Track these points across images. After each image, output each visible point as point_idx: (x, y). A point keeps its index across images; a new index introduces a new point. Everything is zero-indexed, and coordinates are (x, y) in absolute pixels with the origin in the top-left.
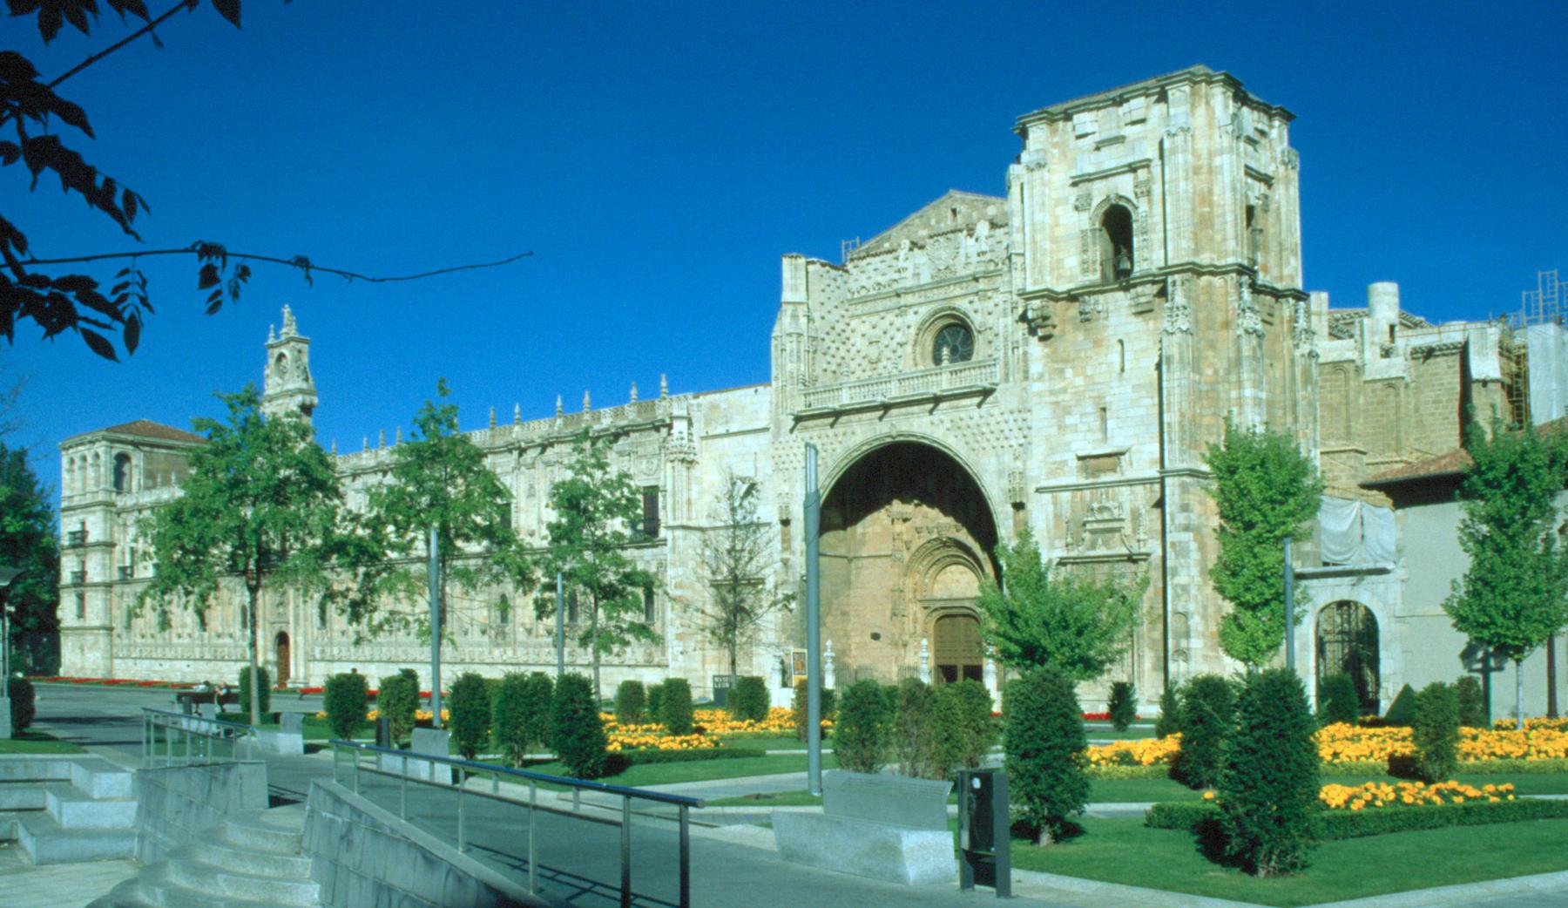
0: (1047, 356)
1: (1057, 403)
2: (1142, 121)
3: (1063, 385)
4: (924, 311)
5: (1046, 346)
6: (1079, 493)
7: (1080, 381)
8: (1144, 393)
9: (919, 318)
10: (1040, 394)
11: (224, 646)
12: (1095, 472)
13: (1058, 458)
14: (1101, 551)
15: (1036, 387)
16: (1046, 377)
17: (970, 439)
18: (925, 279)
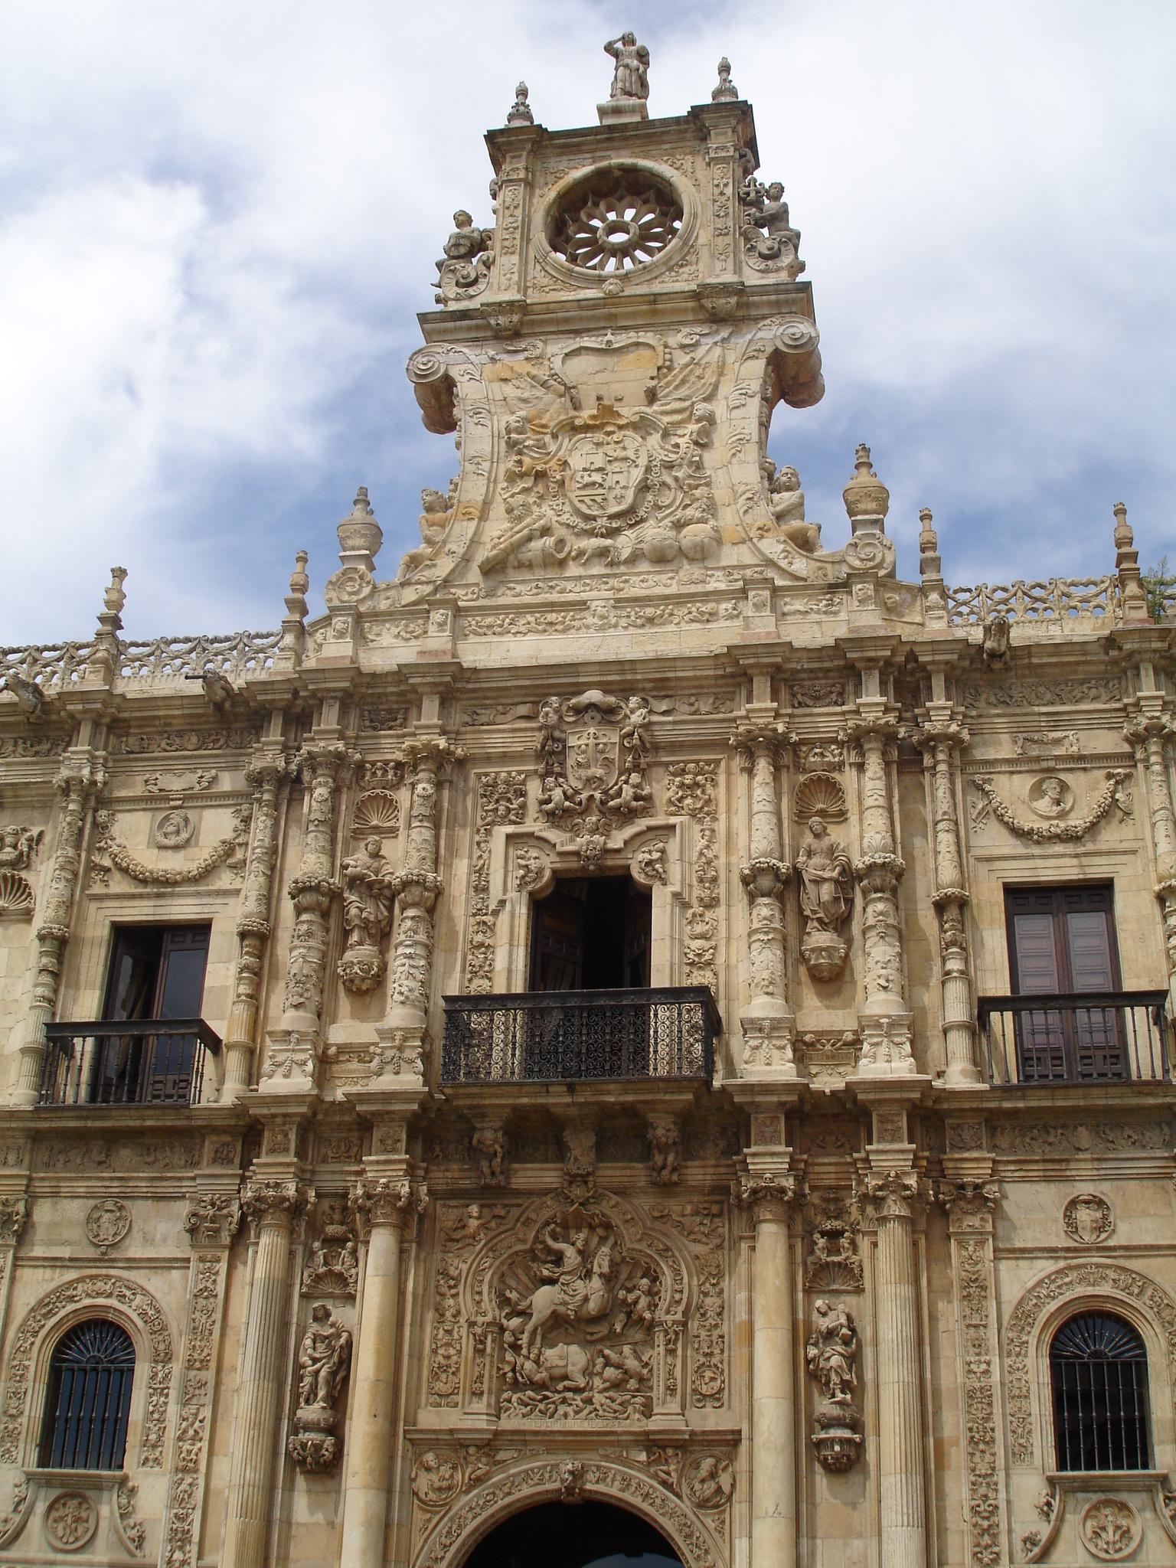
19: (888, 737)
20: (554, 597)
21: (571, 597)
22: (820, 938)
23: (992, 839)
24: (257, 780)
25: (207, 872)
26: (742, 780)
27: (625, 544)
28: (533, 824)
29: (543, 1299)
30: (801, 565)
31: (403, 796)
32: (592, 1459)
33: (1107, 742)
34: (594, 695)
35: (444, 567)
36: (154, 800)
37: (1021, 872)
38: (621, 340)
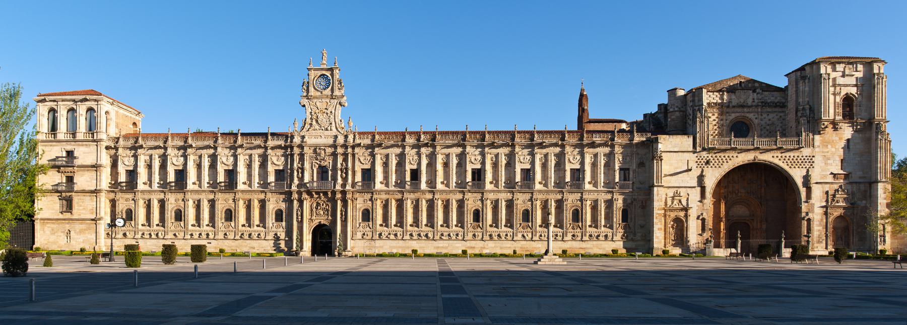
0: (821, 140)
1: (825, 156)
3: (827, 150)
4: (733, 116)
5: (821, 137)
6: (832, 185)
7: (833, 150)
8: (857, 156)
9: (731, 118)
10: (818, 152)
11: (255, 231)
13: (824, 173)
15: (817, 149)
16: (821, 146)
17: (790, 164)
18: (734, 103)
34: (322, 147)
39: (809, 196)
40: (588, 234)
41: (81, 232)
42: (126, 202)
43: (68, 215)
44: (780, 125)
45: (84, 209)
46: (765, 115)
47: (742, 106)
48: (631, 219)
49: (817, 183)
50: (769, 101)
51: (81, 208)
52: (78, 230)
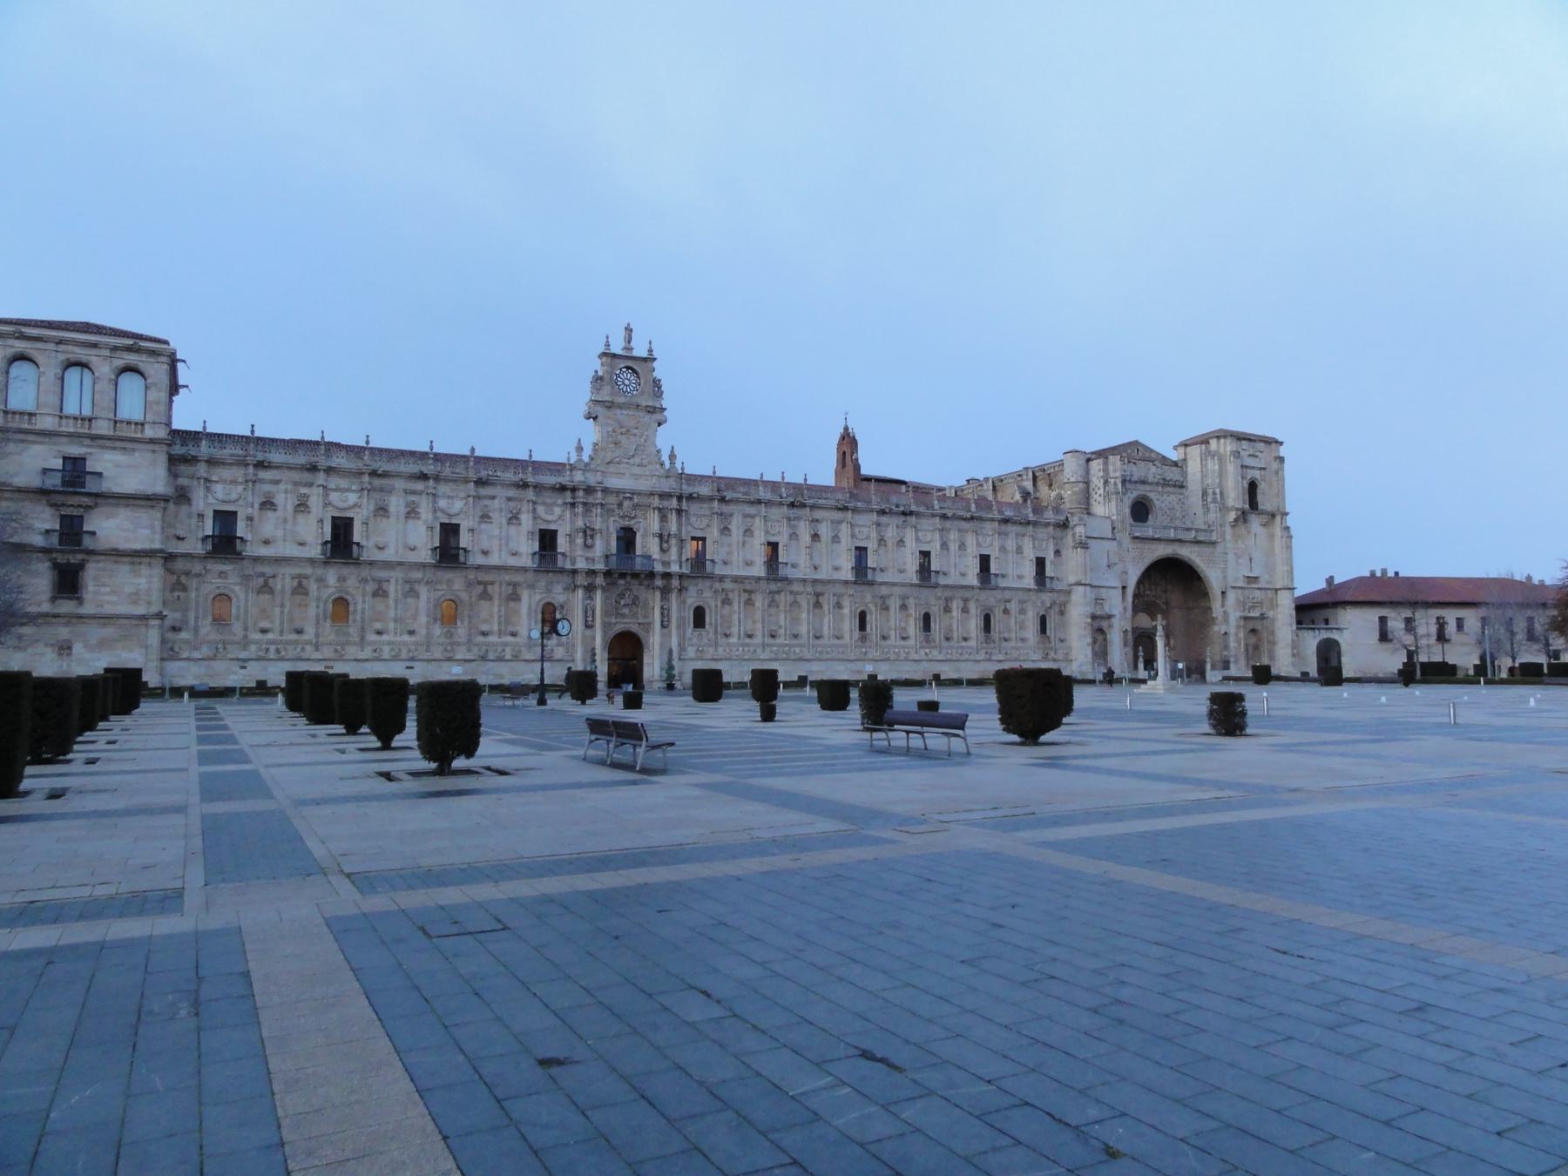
2: (1262, 452)
11: (505, 644)
12: (1249, 583)
14: (1252, 614)
19: (676, 509)
20: (619, 471)
21: (622, 472)
22: (665, 545)
23: (690, 528)
24: (565, 503)
25: (557, 521)
26: (652, 514)
27: (631, 461)
28: (617, 518)
29: (622, 603)
30: (662, 471)
31: (594, 510)
32: (631, 625)
33: (707, 512)
34: (628, 495)
35: (599, 462)
36: (544, 504)
37: (693, 535)
38: (631, 413)
39: (1223, 606)
40: (1003, 652)
41: (103, 644)
42: (221, 581)
43: (66, 607)
44: (1180, 510)
45: (113, 592)
46: (1165, 496)
47: (1143, 482)
48: (1051, 630)
49: (1234, 588)
50: (1168, 478)
51: (108, 589)
52: (93, 641)
